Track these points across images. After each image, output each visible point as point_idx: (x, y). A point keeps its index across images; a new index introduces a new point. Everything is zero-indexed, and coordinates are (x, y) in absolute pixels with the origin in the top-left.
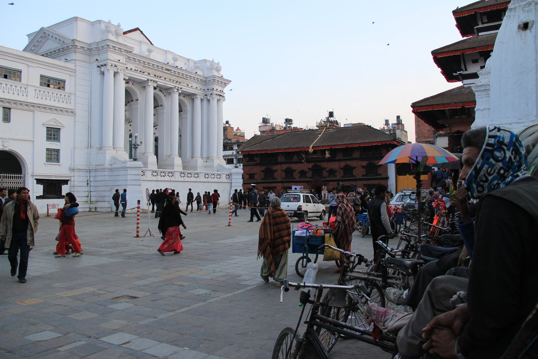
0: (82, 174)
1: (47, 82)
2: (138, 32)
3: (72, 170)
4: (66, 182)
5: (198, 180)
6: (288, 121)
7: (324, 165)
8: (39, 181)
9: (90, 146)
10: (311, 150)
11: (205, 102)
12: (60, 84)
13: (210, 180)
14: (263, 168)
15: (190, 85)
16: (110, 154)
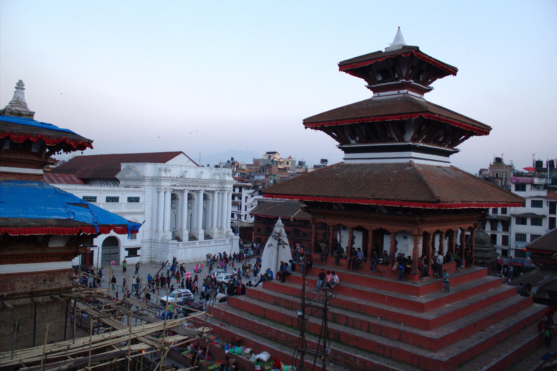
0: (147, 244)
1: (130, 200)
2: (182, 154)
3: (142, 242)
4: (139, 248)
5: (210, 245)
6: (324, 161)
7: (301, 229)
8: (126, 249)
9: (152, 230)
10: (292, 220)
11: (221, 195)
12: (137, 200)
13: (218, 244)
14: (266, 226)
15: (211, 186)
16: (161, 234)
